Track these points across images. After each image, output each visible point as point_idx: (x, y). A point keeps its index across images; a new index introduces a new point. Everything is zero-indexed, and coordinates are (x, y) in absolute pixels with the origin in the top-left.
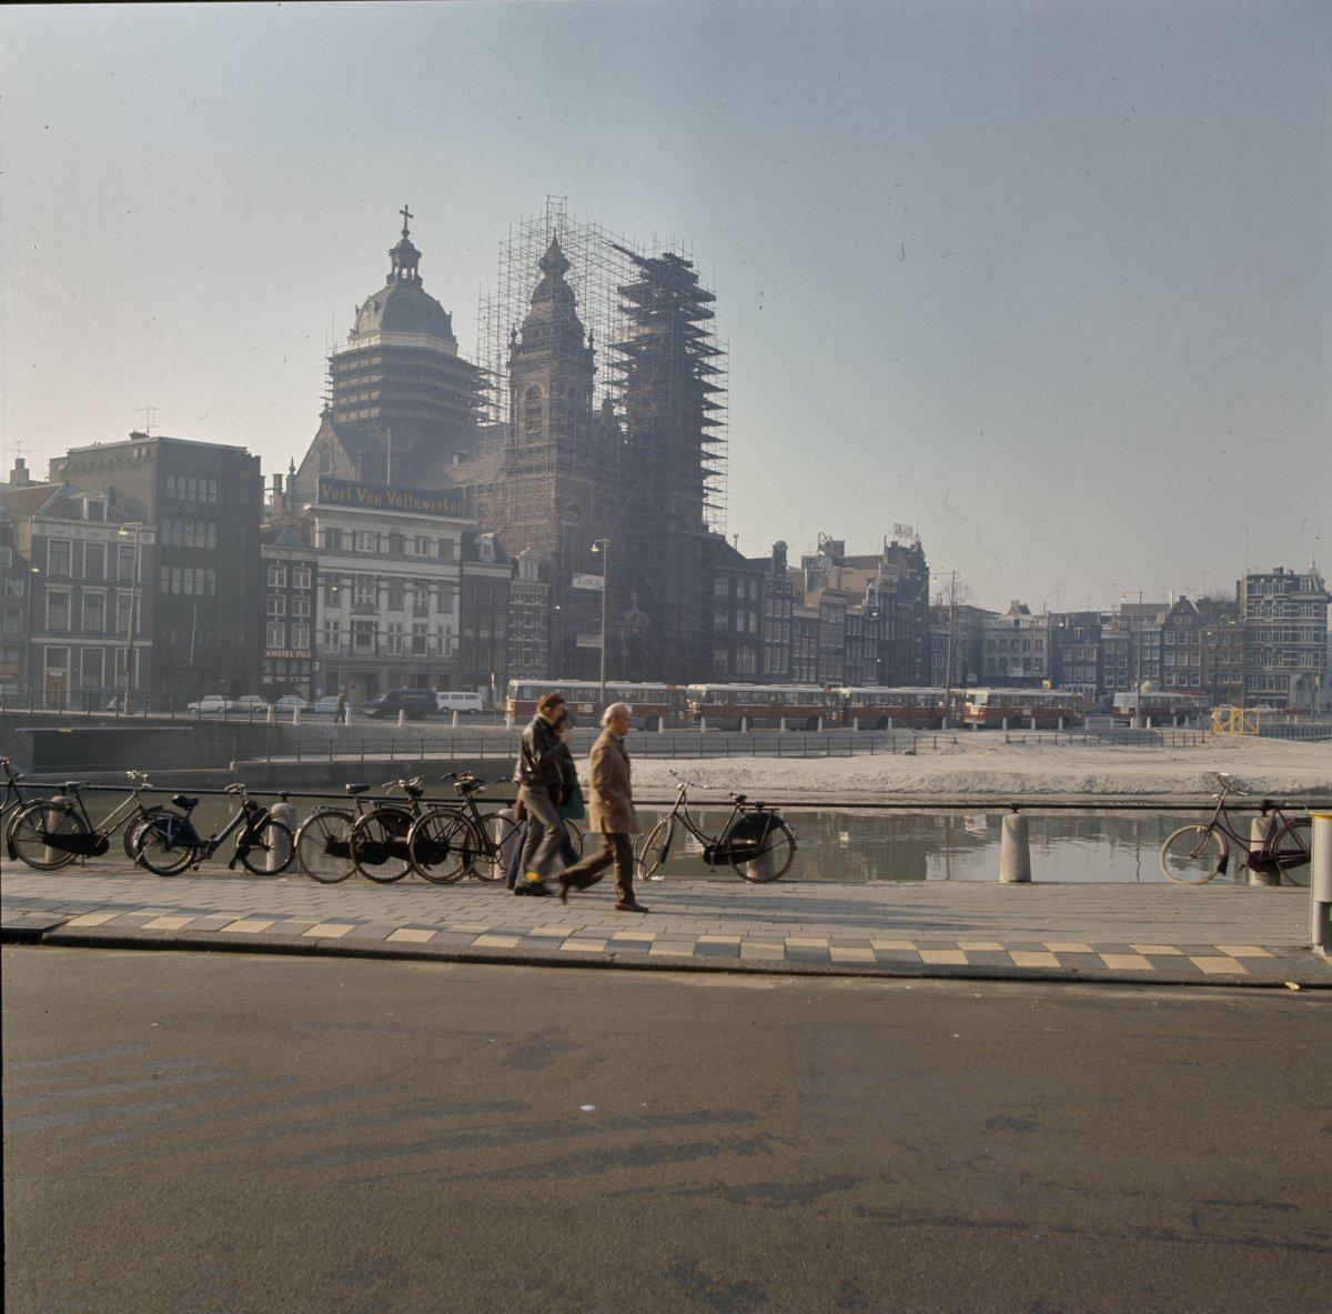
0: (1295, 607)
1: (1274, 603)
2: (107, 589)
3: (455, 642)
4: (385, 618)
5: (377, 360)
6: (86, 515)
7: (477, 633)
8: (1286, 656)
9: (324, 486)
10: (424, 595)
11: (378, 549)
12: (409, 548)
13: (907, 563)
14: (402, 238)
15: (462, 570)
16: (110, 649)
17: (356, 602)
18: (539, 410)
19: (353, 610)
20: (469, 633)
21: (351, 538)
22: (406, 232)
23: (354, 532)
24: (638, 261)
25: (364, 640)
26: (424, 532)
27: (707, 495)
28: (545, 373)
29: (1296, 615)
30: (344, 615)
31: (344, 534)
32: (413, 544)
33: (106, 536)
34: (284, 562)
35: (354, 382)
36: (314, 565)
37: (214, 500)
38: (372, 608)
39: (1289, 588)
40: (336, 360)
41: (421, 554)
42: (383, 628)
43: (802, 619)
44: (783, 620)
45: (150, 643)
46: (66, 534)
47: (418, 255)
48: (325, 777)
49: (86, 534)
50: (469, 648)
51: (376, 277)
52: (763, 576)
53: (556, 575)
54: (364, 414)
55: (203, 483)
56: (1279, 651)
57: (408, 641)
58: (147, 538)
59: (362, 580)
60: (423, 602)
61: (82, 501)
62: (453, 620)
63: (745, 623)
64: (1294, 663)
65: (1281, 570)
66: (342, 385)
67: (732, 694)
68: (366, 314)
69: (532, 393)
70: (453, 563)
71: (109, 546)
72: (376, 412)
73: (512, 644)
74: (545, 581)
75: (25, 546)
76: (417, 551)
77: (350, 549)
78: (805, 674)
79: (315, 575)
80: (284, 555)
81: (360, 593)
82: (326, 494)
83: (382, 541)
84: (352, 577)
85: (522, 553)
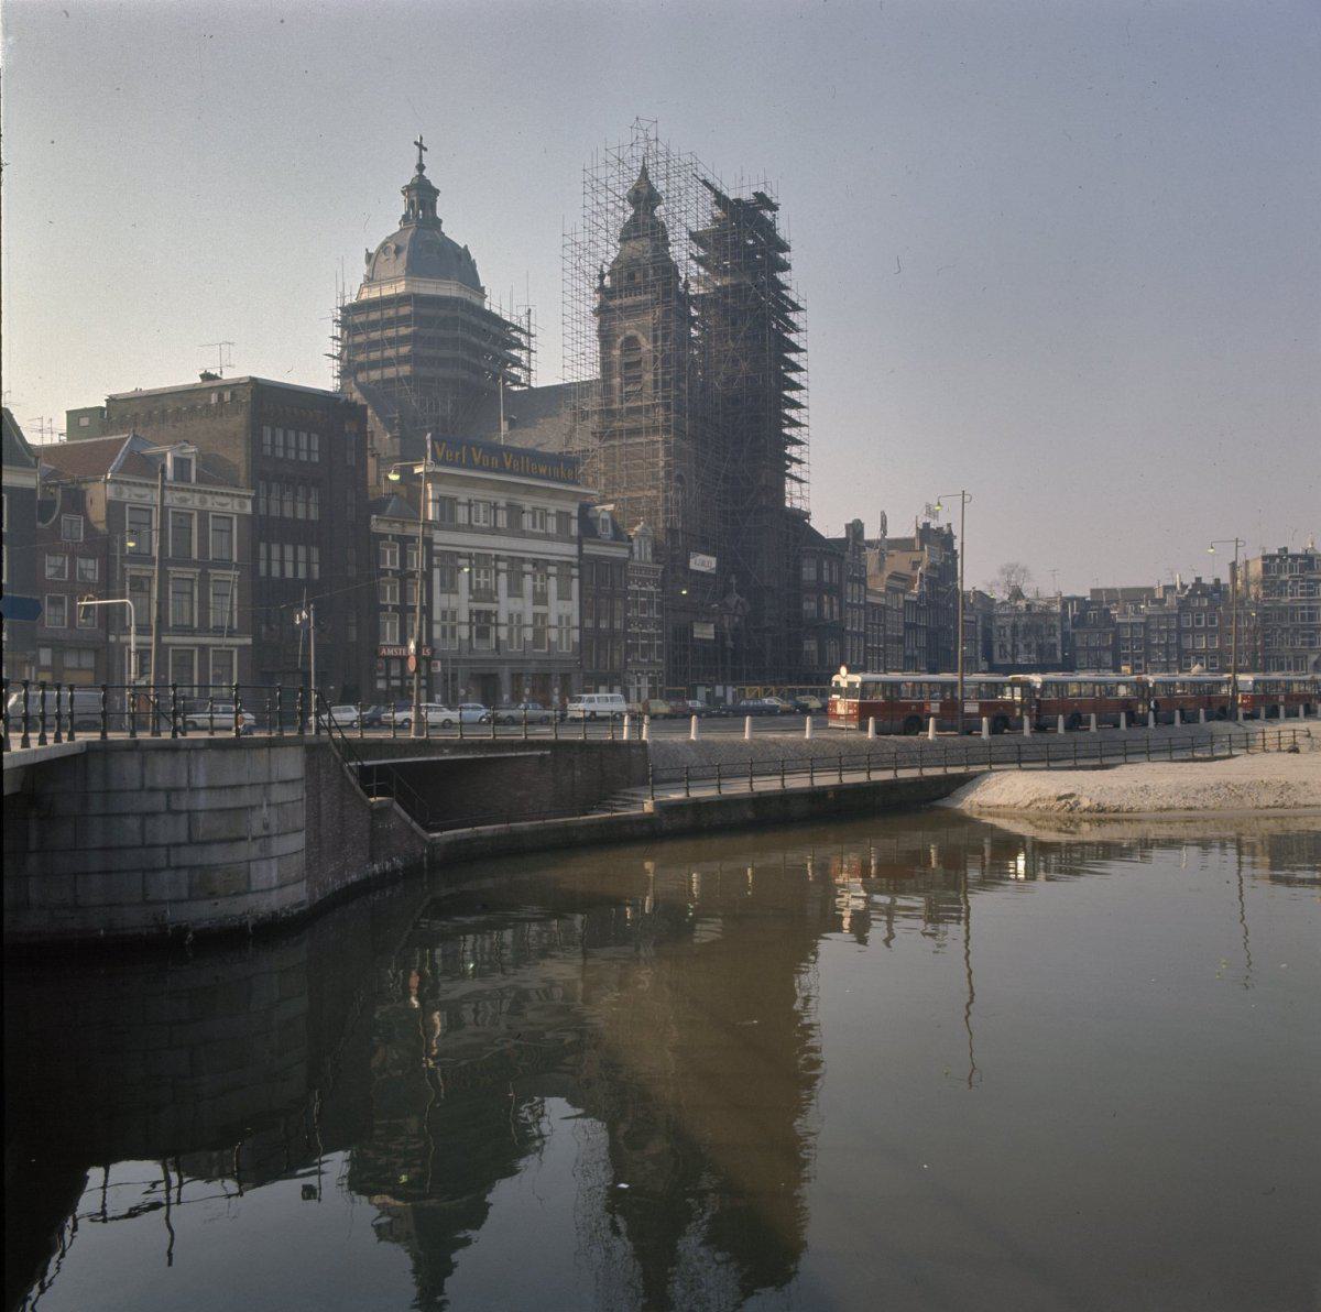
1: (1290, 583)
2: (198, 570)
3: (575, 635)
4: (505, 606)
5: (405, 310)
6: (170, 474)
7: (597, 623)
8: (1304, 636)
9: (436, 443)
10: (542, 580)
11: (495, 523)
12: (527, 522)
13: (939, 541)
15: (580, 549)
16: (203, 648)
17: (474, 588)
18: (639, 363)
19: (471, 597)
20: (589, 623)
22: (421, 167)
23: (470, 500)
24: (721, 200)
25: (483, 633)
26: (540, 502)
27: (788, 467)
28: (648, 320)
29: (1311, 594)
30: (462, 603)
31: (459, 504)
32: (530, 516)
33: (194, 501)
35: (375, 335)
36: (428, 542)
38: (490, 595)
39: (1303, 568)
40: (347, 311)
41: (538, 530)
42: (503, 618)
43: (872, 604)
45: (249, 641)
46: (148, 499)
47: (437, 192)
48: (750, 814)
49: (172, 499)
50: (592, 640)
51: (388, 217)
52: (843, 558)
53: (671, 556)
54: (390, 372)
55: (304, 437)
56: (1296, 631)
57: (529, 634)
58: (242, 506)
59: (481, 561)
60: (542, 587)
61: (164, 455)
62: (572, 608)
63: (830, 609)
64: (1311, 643)
65: (1285, 549)
66: (359, 339)
67: (895, 685)
68: (384, 257)
69: (631, 343)
70: (570, 540)
71: (199, 514)
72: (405, 370)
73: (629, 635)
74: (658, 562)
75: (97, 512)
76: (534, 526)
77: (467, 522)
79: (430, 554)
80: (396, 529)
81: (478, 577)
82: (440, 454)
83: (499, 512)
84: (469, 556)
85: (637, 529)
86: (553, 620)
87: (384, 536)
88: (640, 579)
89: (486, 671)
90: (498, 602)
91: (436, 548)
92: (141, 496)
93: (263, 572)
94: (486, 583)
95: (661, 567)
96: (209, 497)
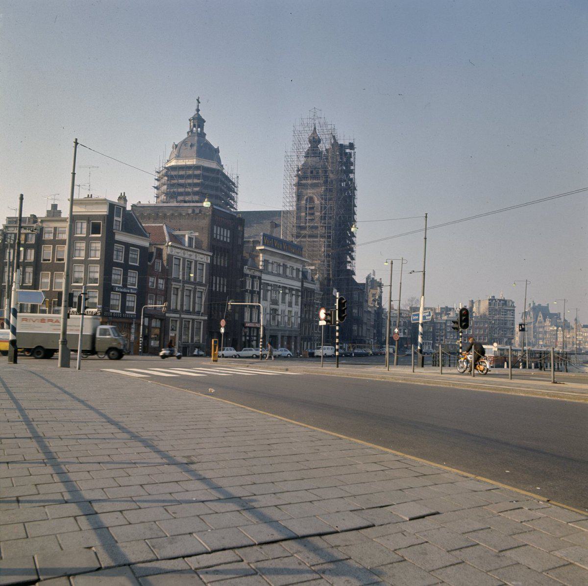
4: (281, 307)
5: (197, 172)
14: (196, 113)
15: (302, 284)
16: (193, 320)
22: (198, 110)
29: (505, 315)
31: (269, 263)
36: (260, 278)
37: (228, 241)
39: (503, 304)
45: (206, 318)
59: (276, 287)
61: (184, 236)
65: (494, 297)
69: (311, 199)
74: (321, 291)
89: (274, 334)
91: (262, 281)
95: (322, 293)
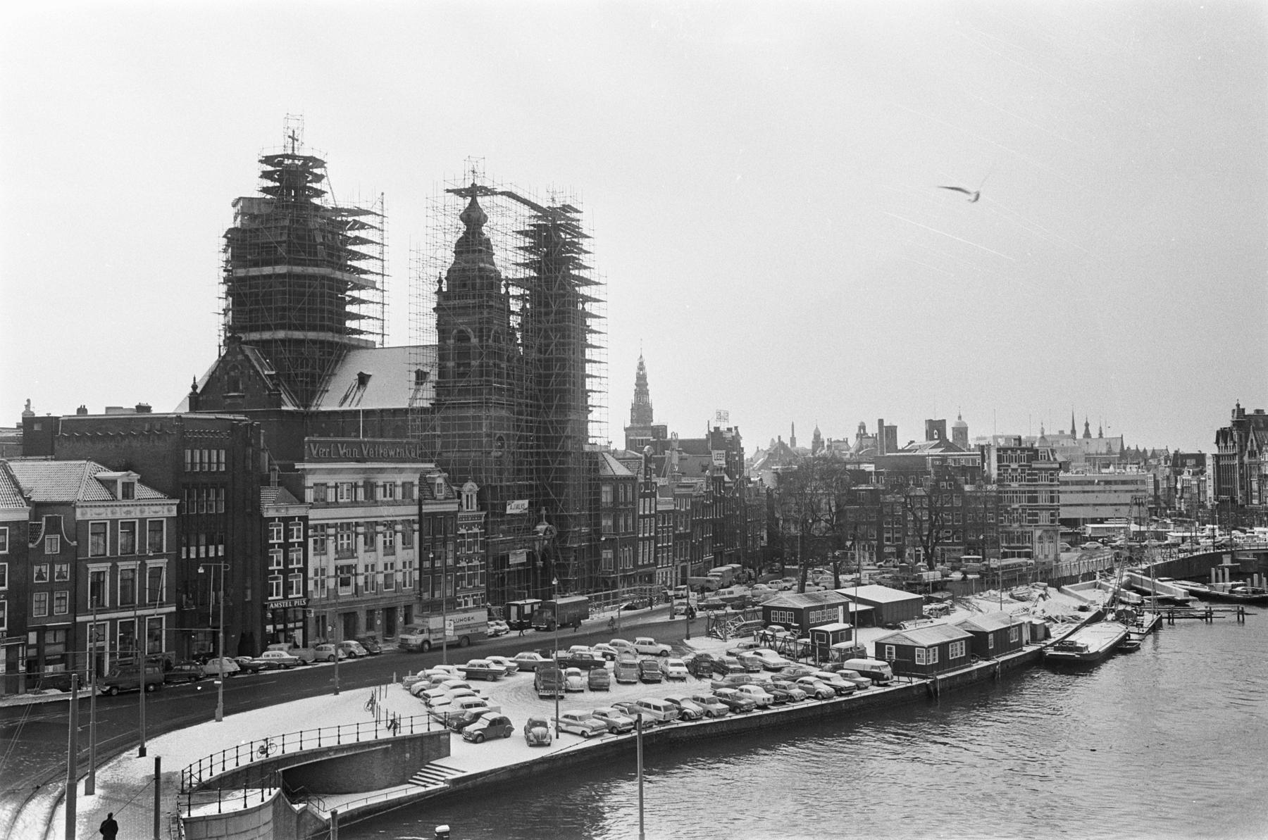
0: (1036, 474)
3: (416, 575)
11: (355, 498)
12: (379, 494)
15: (420, 509)
19: (337, 556)
21: (334, 490)
23: (336, 484)
26: (388, 478)
30: (330, 561)
32: (382, 489)
34: (282, 519)
36: (305, 519)
37: (223, 468)
38: (352, 553)
41: (388, 498)
42: (361, 569)
44: (650, 516)
45: (174, 609)
50: (429, 577)
59: (345, 528)
60: (391, 541)
62: (413, 554)
69: (463, 337)
71: (139, 522)
76: (385, 496)
77: (334, 500)
78: (665, 561)
84: (335, 526)
86: (399, 566)
87: (273, 519)
88: (466, 525)
89: (347, 611)
90: (357, 557)
91: (310, 522)
92: (99, 514)
93: (184, 557)
94: (348, 544)
96: (146, 508)
